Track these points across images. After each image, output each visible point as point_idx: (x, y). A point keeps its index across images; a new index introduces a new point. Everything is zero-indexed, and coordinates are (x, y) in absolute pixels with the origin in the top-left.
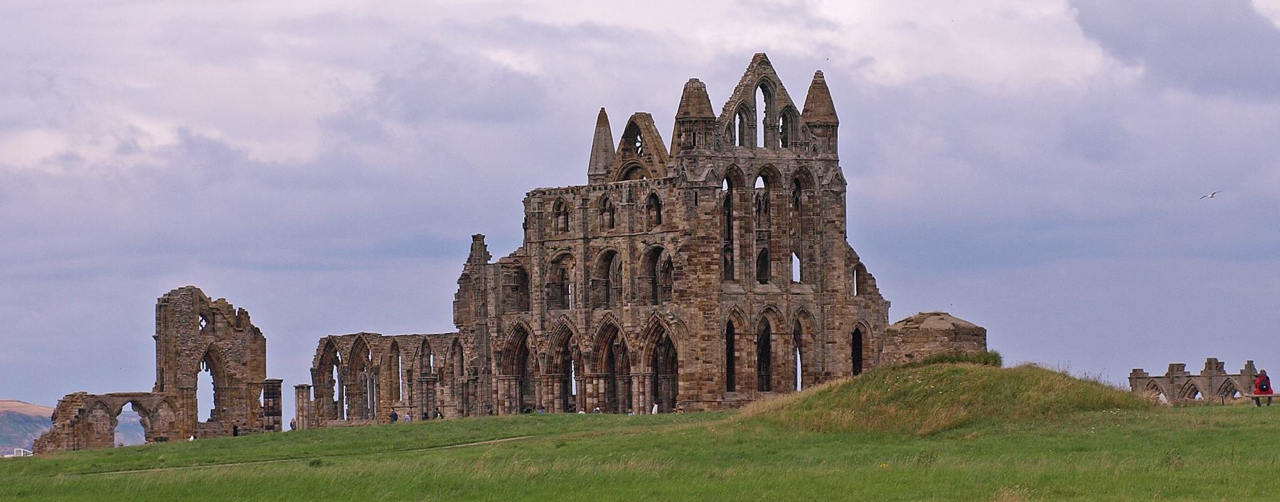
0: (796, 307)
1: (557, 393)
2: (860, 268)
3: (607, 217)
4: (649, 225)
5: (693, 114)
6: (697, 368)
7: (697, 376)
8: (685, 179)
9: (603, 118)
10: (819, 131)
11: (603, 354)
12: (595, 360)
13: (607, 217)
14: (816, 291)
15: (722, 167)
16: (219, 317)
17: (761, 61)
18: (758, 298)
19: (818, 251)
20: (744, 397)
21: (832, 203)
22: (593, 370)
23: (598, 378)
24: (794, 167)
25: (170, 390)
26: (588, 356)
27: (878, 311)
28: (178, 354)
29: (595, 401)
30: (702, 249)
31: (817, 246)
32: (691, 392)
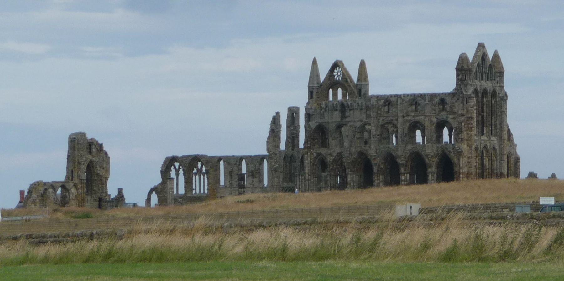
1: (381, 180)
3: (414, 107)
4: (440, 112)
5: (466, 67)
6: (465, 170)
8: (462, 93)
9: (315, 62)
11: (409, 163)
12: (406, 166)
13: (414, 107)
16: (94, 146)
22: (405, 170)
23: (407, 173)
24: (492, 89)
25: (76, 180)
26: (403, 164)
28: (79, 163)
29: (406, 183)
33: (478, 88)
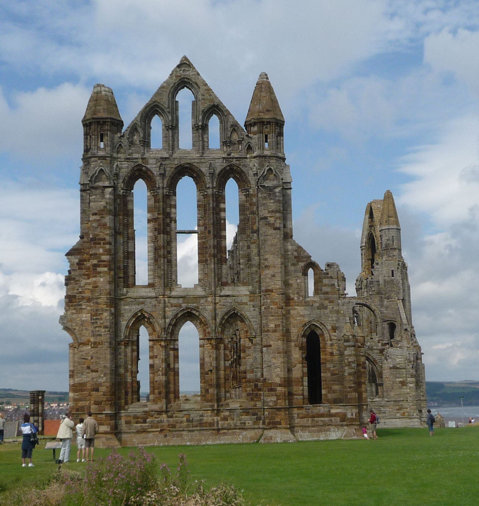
0: (225, 310)
2: (313, 265)
7: (89, 386)
10: (255, 129)
14: (252, 293)
15: (125, 168)
17: (185, 64)
18: (173, 301)
19: (254, 250)
20: (156, 407)
21: (265, 198)
24: (219, 166)
27: (338, 312)
30: (92, 252)
31: (253, 246)
32: (80, 404)
33: (153, 167)
